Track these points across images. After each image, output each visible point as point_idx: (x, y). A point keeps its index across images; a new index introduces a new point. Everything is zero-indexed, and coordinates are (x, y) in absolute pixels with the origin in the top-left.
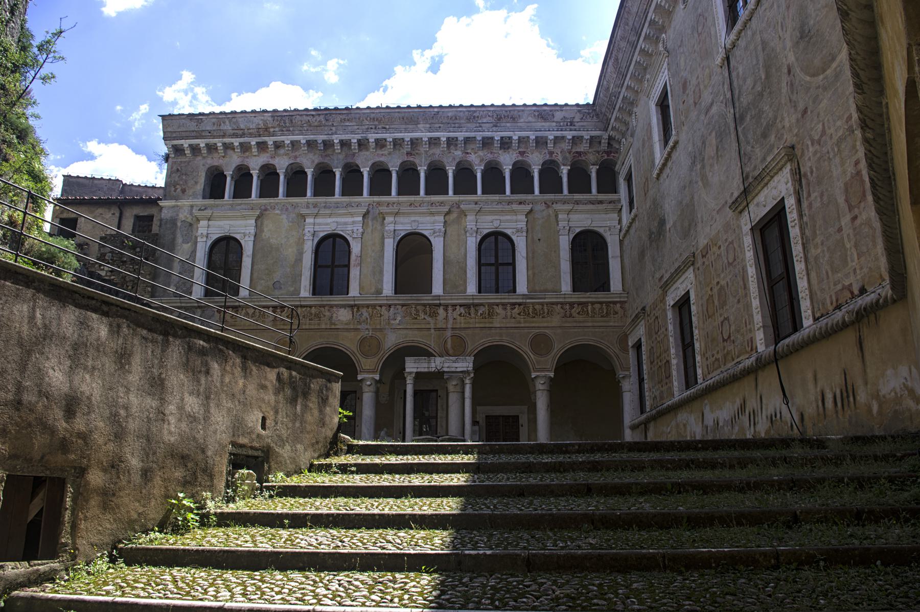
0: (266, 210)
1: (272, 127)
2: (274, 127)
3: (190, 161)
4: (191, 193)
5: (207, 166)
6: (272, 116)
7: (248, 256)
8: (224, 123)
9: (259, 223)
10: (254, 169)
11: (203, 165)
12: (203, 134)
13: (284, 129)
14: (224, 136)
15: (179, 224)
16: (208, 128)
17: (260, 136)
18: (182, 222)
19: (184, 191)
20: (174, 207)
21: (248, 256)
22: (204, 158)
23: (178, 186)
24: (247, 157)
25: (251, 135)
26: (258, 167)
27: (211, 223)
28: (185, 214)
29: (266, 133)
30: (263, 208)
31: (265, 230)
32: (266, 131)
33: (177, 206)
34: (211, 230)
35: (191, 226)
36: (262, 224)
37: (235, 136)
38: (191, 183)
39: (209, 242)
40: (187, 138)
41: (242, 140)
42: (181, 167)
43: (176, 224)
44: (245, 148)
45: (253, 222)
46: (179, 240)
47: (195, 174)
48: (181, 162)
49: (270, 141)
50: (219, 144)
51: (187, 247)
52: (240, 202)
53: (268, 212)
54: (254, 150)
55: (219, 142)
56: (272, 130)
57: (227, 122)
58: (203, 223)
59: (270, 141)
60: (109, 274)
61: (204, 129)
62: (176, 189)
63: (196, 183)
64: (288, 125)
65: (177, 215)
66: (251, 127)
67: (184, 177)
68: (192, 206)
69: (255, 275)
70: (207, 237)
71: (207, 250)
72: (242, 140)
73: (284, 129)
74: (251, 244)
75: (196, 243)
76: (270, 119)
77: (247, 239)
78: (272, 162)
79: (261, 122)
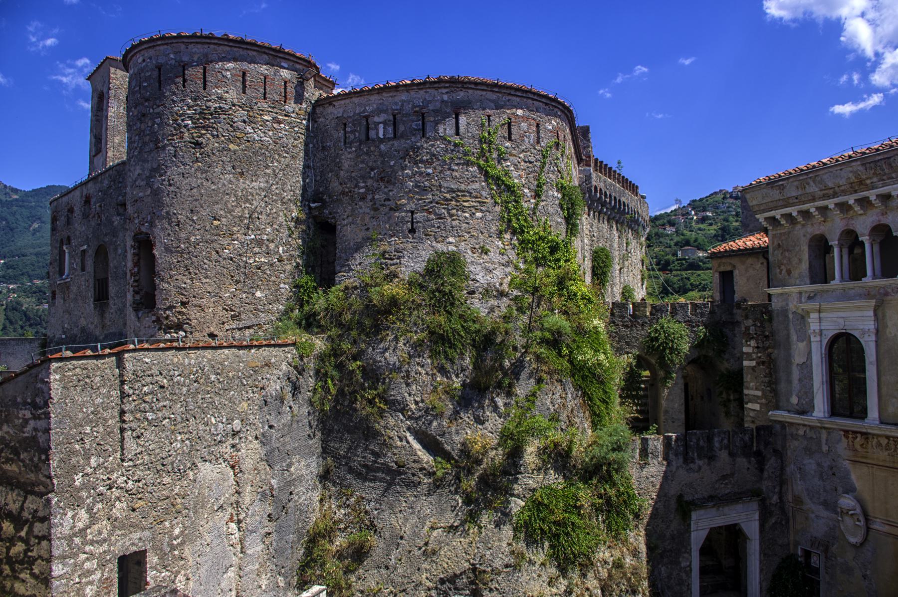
0: (887, 294)
1: (867, 178)
2: (870, 178)
3: (789, 232)
4: (796, 275)
5: (809, 237)
6: (862, 165)
7: (871, 363)
8: (808, 184)
9: (880, 314)
10: (863, 235)
11: (804, 236)
12: (791, 201)
13: (885, 177)
14: (814, 200)
15: (791, 316)
16: (794, 194)
17: (856, 192)
18: (793, 313)
19: (789, 272)
20: (782, 294)
21: (871, 363)
22: (803, 225)
23: (783, 267)
24: (852, 218)
25: (844, 192)
26: (867, 232)
27: (822, 315)
28: (795, 303)
29: (861, 187)
30: (882, 291)
31: (890, 324)
32: (860, 184)
33: (786, 293)
34: (825, 325)
35: (803, 318)
36: (884, 316)
37: (826, 197)
38: (795, 261)
39: (825, 342)
40: (776, 208)
41: (836, 200)
42: (782, 241)
43: (787, 316)
44: (844, 207)
45: (871, 313)
46: (794, 337)
47: (797, 249)
48: (781, 234)
49: (872, 195)
50: (812, 210)
51: (802, 345)
52: (852, 285)
53: (889, 298)
54: (857, 208)
55: (811, 207)
56: (868, 182)
57: (812, 183)
58: (814, 316)
59: (872, 195)
60: (756, 350)
61: (789, 196)
62: (781, 270)
63: (800, 261)
64: (886, 171)
65: (787, 305)
66: (841, 184)
67: (787, 254)
68: (800, 293)
69: (884, 390)
70: (821, 335)
71: (823, 352)
72: (836, 200)
73: (885, 177)
74: (872, 345)
75: (810, 342)
76: (860, 168)
77: (866, 338)
78: (884, 221)
79: (851, 175)
